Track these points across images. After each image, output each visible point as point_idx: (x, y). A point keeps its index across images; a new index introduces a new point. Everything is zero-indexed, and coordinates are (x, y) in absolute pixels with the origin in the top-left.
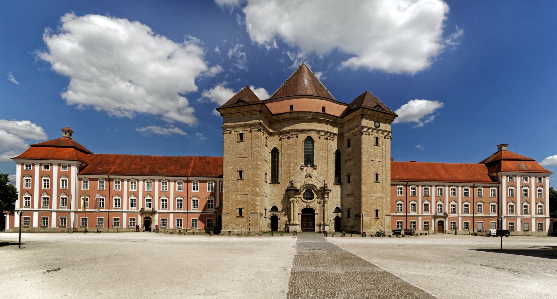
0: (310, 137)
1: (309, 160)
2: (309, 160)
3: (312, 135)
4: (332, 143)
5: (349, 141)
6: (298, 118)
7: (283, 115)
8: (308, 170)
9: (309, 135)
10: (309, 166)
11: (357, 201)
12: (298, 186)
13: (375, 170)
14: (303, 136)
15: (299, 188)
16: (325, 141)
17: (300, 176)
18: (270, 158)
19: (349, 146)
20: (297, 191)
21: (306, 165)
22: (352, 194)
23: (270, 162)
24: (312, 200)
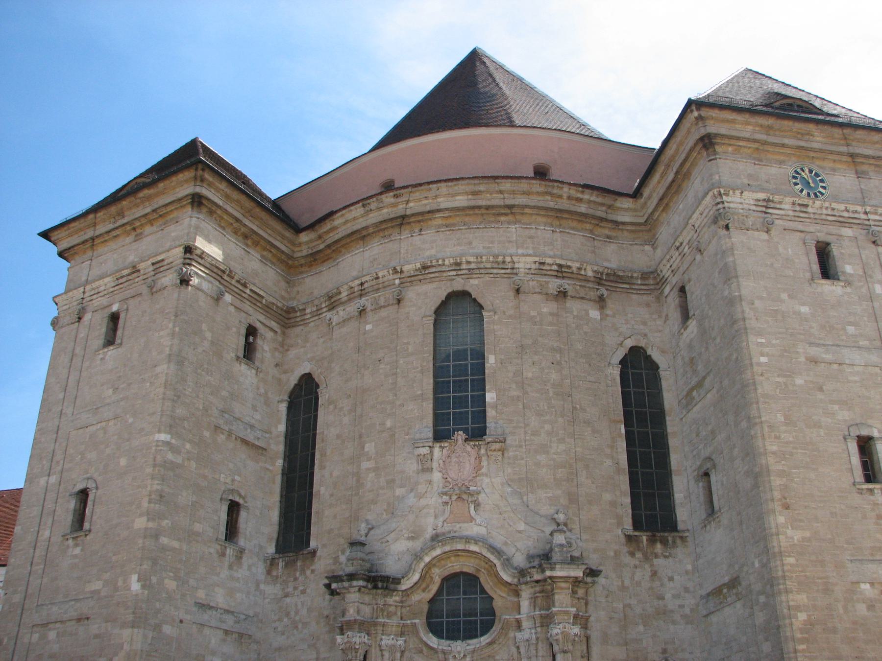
0: (464, 295)
1: (459, 407)
2: (459, 407)
3: (473, 285)
4: (595, 314)
5: (682, 290)
6: (402, 221)
7: (338, 221)
8: (459, 457)
9: (458, 285)
10: (460, 436)
11: (760, 618)
12: (396, 552)
13: (844, 415)
14: (425, 298)
15: (391, 567)
16: (548, 307)
17: (411, 500)
18: (282, 428)
19: (686, 316)
20: (379, 582)
21: (440, 435)
22: (734, 583)
23: (278, 447)
24: (484, 639)
